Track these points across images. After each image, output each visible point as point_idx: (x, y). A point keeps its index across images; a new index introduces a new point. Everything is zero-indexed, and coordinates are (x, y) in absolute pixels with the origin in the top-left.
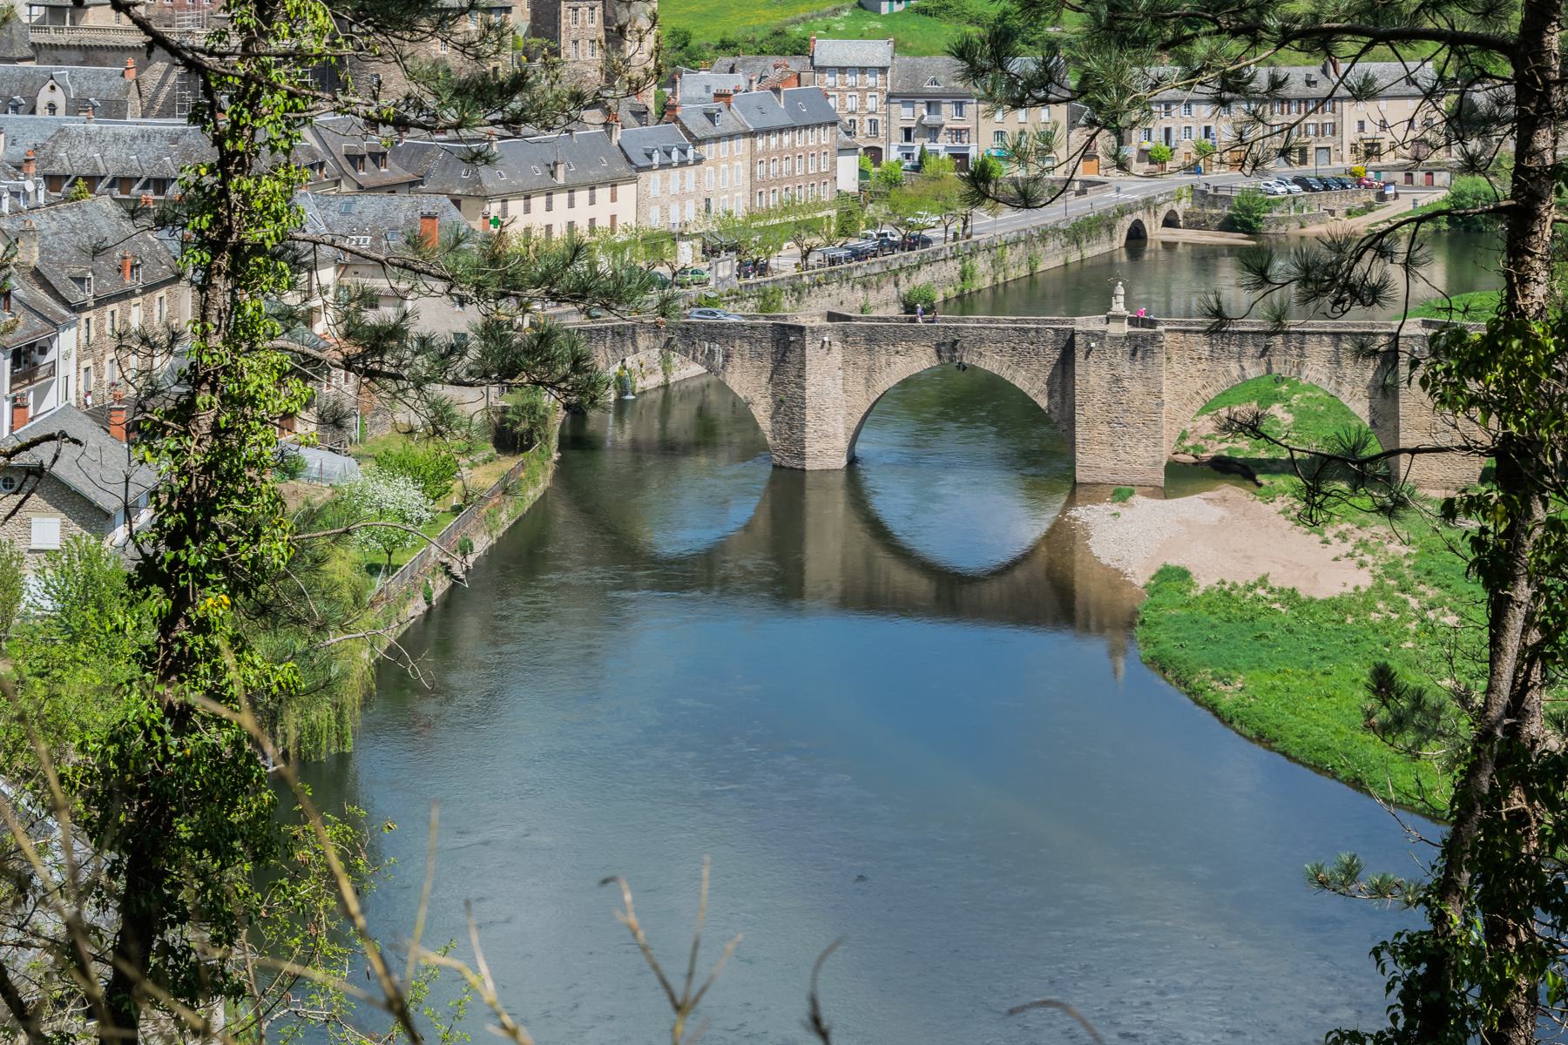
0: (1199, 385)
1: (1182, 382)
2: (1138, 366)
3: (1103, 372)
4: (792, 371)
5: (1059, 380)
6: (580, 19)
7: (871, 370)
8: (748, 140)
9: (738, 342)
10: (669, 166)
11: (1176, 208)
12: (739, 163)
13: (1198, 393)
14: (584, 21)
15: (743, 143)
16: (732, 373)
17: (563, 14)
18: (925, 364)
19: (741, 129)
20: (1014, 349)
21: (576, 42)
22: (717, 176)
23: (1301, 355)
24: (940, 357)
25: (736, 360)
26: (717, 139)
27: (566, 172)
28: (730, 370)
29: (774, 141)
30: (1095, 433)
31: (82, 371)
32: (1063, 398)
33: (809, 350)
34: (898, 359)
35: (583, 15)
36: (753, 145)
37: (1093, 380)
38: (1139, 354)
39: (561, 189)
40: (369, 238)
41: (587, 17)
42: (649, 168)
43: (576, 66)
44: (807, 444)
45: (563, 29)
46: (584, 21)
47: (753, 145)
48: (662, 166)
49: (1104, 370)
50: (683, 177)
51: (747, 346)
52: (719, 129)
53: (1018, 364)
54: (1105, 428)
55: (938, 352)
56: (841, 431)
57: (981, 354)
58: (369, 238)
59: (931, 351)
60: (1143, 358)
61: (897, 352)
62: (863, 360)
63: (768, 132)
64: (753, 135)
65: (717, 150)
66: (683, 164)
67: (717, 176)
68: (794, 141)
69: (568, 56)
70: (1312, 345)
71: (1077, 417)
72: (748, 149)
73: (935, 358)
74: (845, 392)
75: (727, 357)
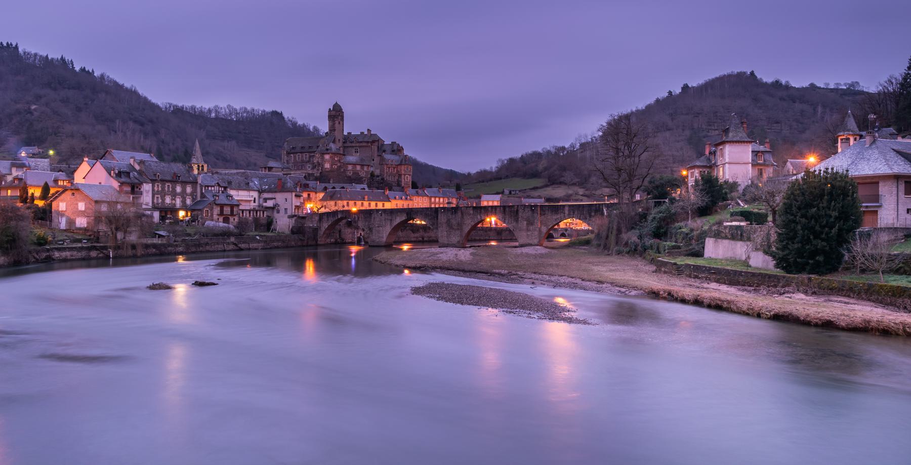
2: (454, 216)
5: (436, 221)
7: (391, 220)
11: (565, 232)
18: (404, 218)
23: (496, 212)
24: (407, 217)
25: (360, 219)
30: (443, 234)
31: (155, 198)
36: (431, 200)
46: (392, 171)
55: (407, 215)
60: (455, 213)
62: (390, 218)
70: (498, 209)
75: (358, 218)
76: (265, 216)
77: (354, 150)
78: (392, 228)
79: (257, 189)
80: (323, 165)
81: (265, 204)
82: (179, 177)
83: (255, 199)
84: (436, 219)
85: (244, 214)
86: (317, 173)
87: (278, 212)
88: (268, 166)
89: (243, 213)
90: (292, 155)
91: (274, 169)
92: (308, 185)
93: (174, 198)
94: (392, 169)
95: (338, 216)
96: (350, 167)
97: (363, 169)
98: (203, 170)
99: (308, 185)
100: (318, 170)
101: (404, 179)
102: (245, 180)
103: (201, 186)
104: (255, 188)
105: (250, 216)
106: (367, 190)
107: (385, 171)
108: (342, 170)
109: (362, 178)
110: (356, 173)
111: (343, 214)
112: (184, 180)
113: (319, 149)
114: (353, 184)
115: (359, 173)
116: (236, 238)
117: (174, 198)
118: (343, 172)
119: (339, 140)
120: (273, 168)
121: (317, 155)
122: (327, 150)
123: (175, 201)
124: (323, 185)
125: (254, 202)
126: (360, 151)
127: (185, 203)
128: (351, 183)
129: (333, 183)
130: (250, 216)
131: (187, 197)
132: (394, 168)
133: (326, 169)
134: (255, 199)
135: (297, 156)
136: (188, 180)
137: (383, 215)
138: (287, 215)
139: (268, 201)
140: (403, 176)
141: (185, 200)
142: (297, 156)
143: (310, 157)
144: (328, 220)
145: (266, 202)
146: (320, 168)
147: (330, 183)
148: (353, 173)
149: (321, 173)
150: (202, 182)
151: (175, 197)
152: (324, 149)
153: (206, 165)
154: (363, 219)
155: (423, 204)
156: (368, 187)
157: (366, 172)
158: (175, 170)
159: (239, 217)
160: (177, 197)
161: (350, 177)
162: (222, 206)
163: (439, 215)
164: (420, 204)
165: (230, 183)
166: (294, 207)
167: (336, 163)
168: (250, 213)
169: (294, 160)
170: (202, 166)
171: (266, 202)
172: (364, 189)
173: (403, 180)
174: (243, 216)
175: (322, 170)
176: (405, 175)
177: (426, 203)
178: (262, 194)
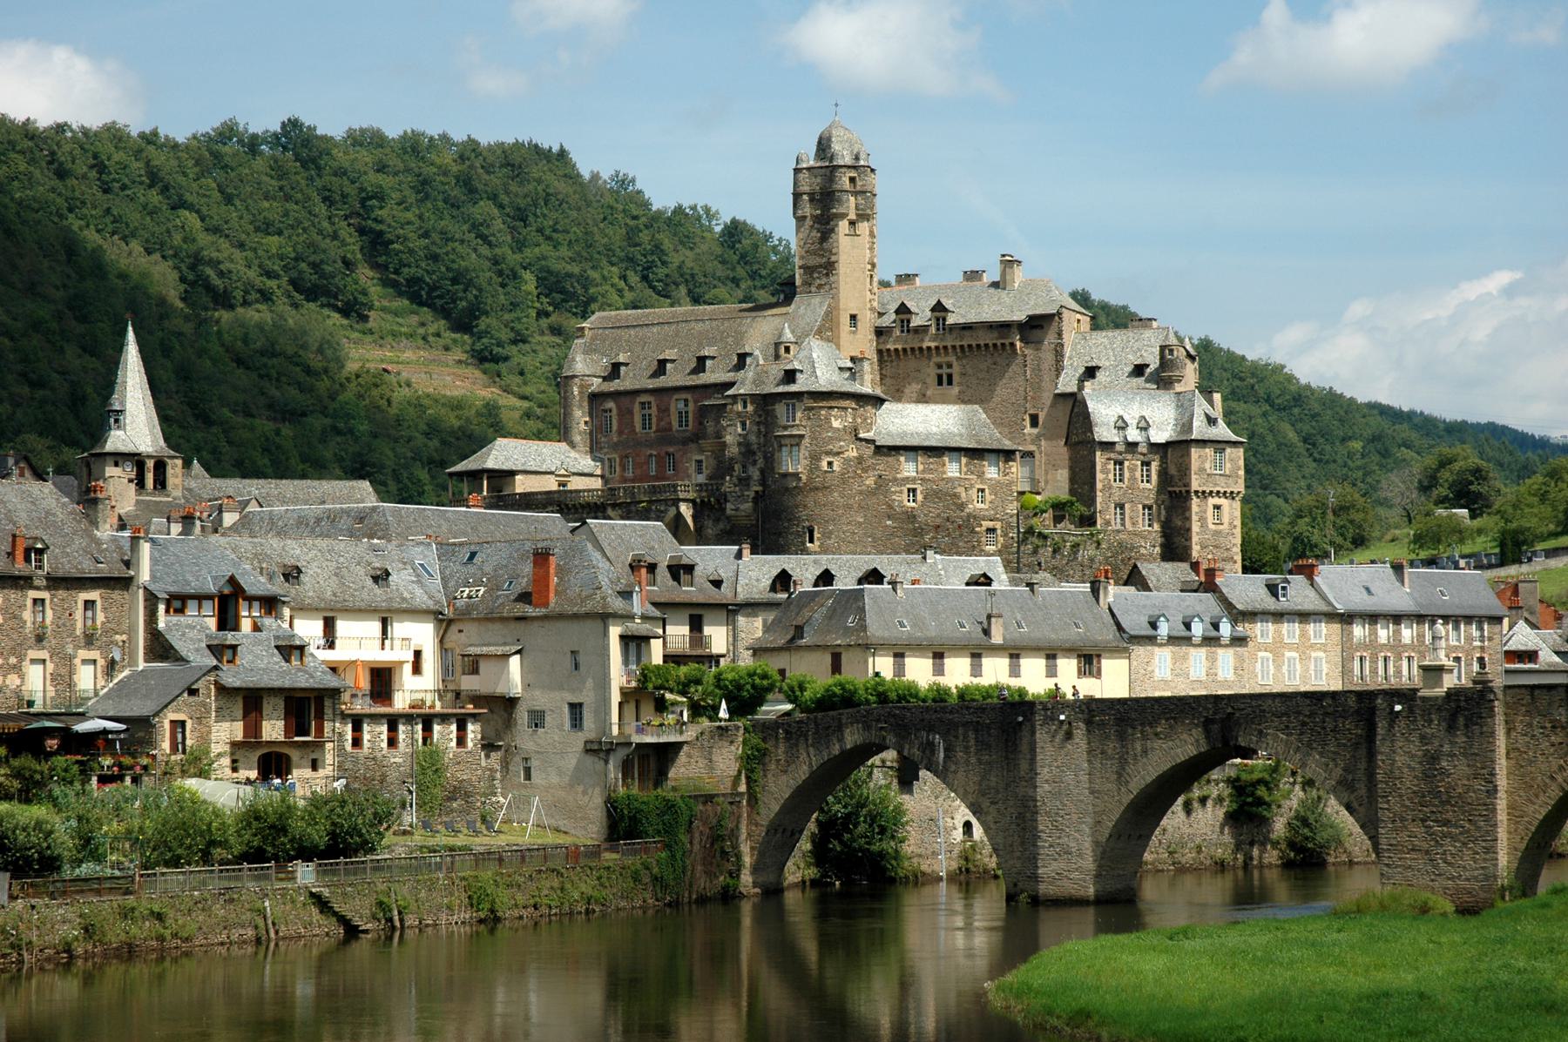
0: (1555, 768)
1: (1531, 762)
2: (1461, 739)
3: (1413, 749)
4: (1024, 765)
6: (1127, 474)
7: (1123, 762)
8: (1336, 627)
9: (961, 730)
10: (1186, 640)
12: (1321, 654)
13: (1552, 778)
14: (1132, 478)
15: (1322, 632)
16: (955, 772)
17: (1098, 467)
19: (1324, 608)
20: (1304, 724)
21: (1122, 507)
22: (1278, 667)
26: (1278, 616)
27: (1006, 627)
28: (953, 768)
29: (1383, 633)
32: (1369, 790)
33: (1041, 736)
34: (1157, 744)
35: (1132, 470)
37: (1400, 759)
38: (1461, 721)
39: (995, 650)
40: (483, 589)
41: (1138, 474)
42: (1151, 640)
43: (1121, 536)
44: (1040, 864)
45: (1099, 486)
46: (1132, 478)
47: (1347, 637)
48: (1173, 640)
49: (1415, 748)
50: (1212, 660)
51: (971, 735)
52: (1284, 603)
53: (1309, 745)
54: (1418, 829)
55: (1207, 732)
56: (1087, 845)
57: (1261, 732)
58: (483, 589)
59: (1198, 733)
60: (1466, 726)
61: (1156, 734)
63: (1373, 618)
64: (1347, 618)
65: (1278, 633)
66: (1211, 641)
67: (1278, 667)
68: (1421, 636)
69: (1108, 523)
71: (1380, 813)
72: (1336, 638)
73: (1203, 741)
74: (1092, 792)
76: (470, 744)
77: (932, 372)
78: (1127, 799)
79: (431, 604)
80: (770, 463)
81: (469, 683)
82: (40, 552)
83: (418, 654)
84: (1363, 752)
85: (366, 737)
86: (741, 498)
87: (537, 719)
88: (491, 464)
89: (357, 728)
90: (611, 405)
91: (518, 477)
92: (690, 569)
93: (13, 660)
94: (1132, 470)
95: (841, 740)
96: (908, 468)
97: (981, 475)
98: (161, 483)
99: (690, 569)
100: (744, 482)
101: (1202, 520)
102: (370, 557)
103: (151, 599)
104: (420, 598)
105: (392, 742)
106: (1001, 581)
107: (1099, 476)
108: (870, 482)
109: (975, 518)
110: (943, 495)
111: (867, 727)
112: (67, 568)
113: (749, 374)
114: (930, 553)
115: (956, 496)
116: (321, 872)
117: (13, 660)
118: (872, 493)
119: (853, 317)
120: (512, 473)
121: (739, 407)
122: (790, 376)
123: (22, 677)
124: (770, 565)
125: (417, 669)
126: (963, 374)
127: (71, 685)
128: (922, 550)
129: (824, 550)
130: (392, 742)
131: (83, 654)
132: (1147, 464)
133: (785, 475)
134: (418, 654)
135: (637, 407)
136: (88, 568)
137: (1080, 732)
138: (579, 740)
139: (483, 666)
140: (1195, 501)
141: (71, 673)
142: (637, 407)
143: (703, 412)
144: (791, 759)
145: (475, 670)
146: (755, 473)
147: (805, 551)
148: (931, 496)
149: (758, 498)
150: (153, 577)
151: (21, 659)
152: (776, 370)
153: (179, 462)
154: (973, 760)
155: (1304, 658)
156: (1014, 566)
157: (996, 487)
158: (22, 517)
159: (341, 748)
160: (32, 654)
161: (910, 516)
162: (251, 701)
163: (1381, 727)
164: (1288, 654)
165: (292, 574)
166: (616, 698)
167: (834, 447)
168: (393, 728)
169: (620, 432)
170: (160, 466)
171: (475, 670)
172: (986, 580)
173: (1195, 527)
174: (357, 742)
175: (763, 482)
176: (1204, 495)
177: (1323, 648)
178: (454, 628)
